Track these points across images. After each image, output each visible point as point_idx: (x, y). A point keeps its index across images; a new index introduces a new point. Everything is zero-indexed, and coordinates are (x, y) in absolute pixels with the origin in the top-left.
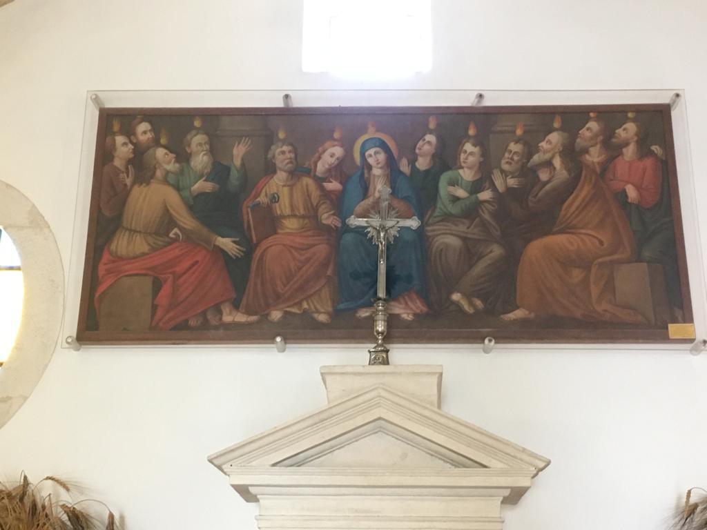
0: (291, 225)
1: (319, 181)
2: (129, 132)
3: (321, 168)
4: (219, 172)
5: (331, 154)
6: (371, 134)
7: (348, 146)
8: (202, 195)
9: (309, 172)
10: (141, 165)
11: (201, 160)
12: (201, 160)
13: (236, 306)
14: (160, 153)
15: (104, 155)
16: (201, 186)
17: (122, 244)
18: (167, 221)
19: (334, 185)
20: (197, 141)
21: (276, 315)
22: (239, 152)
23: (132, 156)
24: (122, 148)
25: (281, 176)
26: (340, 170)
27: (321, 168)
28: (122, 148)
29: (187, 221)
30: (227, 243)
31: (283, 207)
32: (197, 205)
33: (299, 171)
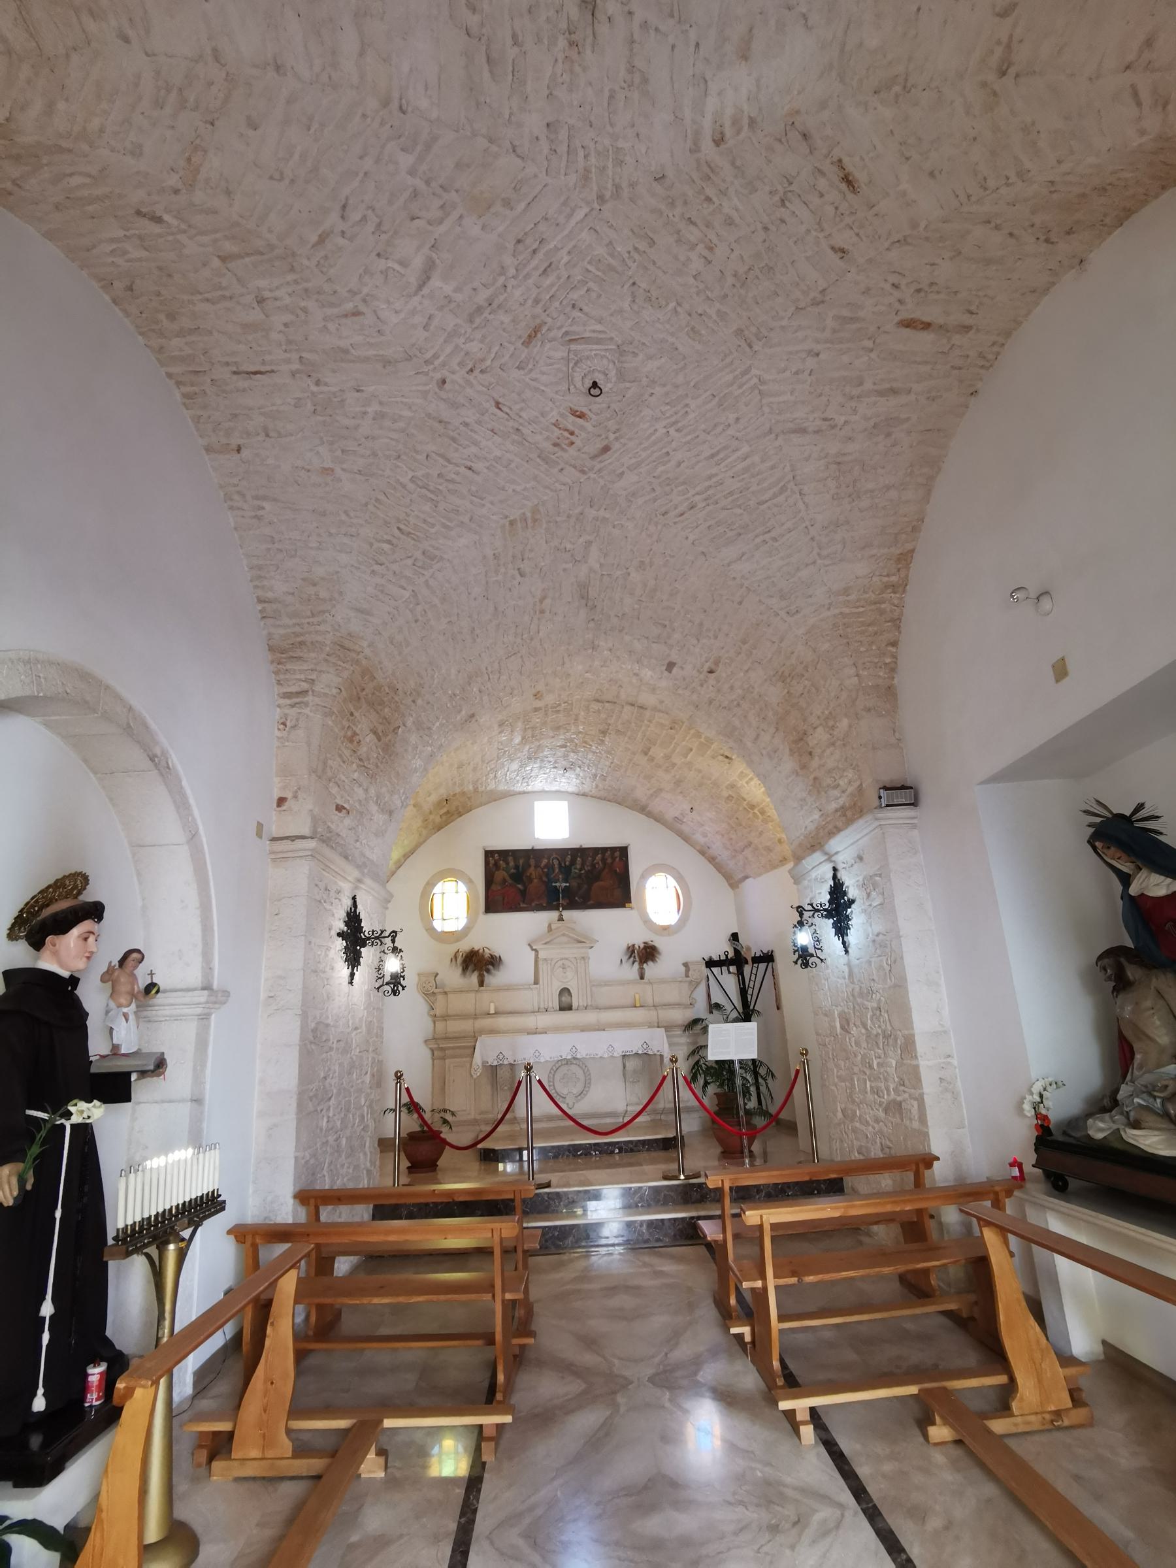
0: (535, 881)
1: (542, 869)
2: (493, 857)
3: (542, 865)
4: (517, 867)
5: (545, 861)
6: (554, 856)
7: (549, 859)
8: (513, 873)
9: (539, 866)
10: (496, 864)
11: (512, 864)
12: (512, 864)
13: (523, 902)
14: (501, 862)
15: (487, 863)
16: (513, 871)
17: (494, 887)
18: (504, 881)
19: (546, 870)
20: (510, 859)
21: (533, 904)
22: (521, 862)
23: (487, 955)
24: (492, 861)
25: (532, 869)
26: (546, 866)
27: (542, 865)
28: (492, 861)
29: (510, 881)
30: (520, 886)
31: (534, 876)
32: (512, 876)
33: (537, 866)
